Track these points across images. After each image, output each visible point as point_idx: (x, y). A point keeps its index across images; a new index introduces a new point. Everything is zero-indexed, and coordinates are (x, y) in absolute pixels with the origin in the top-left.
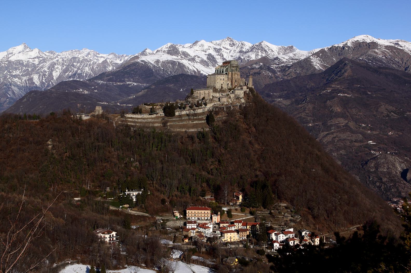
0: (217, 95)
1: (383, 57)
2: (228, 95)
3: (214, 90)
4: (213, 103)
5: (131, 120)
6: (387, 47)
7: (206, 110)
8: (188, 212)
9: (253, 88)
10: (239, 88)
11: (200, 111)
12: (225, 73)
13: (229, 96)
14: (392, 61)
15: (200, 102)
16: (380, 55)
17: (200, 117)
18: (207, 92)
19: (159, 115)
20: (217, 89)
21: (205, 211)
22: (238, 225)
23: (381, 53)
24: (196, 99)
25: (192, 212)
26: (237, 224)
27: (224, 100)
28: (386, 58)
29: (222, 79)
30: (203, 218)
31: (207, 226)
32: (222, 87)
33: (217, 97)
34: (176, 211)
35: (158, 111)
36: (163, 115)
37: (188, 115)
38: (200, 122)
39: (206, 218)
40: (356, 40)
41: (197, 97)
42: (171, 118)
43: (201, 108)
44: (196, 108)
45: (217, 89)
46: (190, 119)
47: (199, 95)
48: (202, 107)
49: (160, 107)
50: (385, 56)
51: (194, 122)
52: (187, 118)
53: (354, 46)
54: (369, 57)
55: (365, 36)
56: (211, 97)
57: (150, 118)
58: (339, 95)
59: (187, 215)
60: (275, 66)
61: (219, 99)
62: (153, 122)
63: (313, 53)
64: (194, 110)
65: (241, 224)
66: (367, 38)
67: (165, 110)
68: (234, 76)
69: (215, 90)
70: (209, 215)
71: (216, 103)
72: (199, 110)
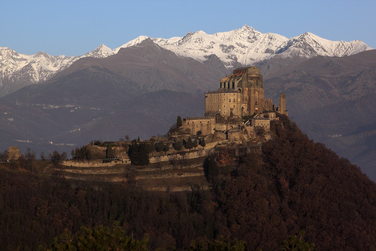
0: (224, 127)
2: (243, 127)
3: (218, 119)
4: (215, 141)
5: (70, 171)
7: (204, 153)
9: (287, 115)
10: (262, 116)
11: (193, 156)
12: (236, 89)
13: (244, 130)
15: (193, 140)
17: (193, 166)
18: (205, 122)
19: (121, 163)
20: (224, 118)
27: (236, 136)
32: (231, 113)
33: (223, 132)
35: (118, 156)
37: (172, 162)
38: (193, 175)
41: (188, 130)
42: (141, 169)
43: (195, 151)
44: (186, 150)
45: (224, 118)
46: (175, 170)
47: (191, 128)
48: (197, 149)
49: (122, 148)
51: (183, 176)
52: (171, 167)
56: (213, 132)
57: (105, 168)
60: (328, 76)
61: (227, 133)
62: (110, 174)
64: (183, 153)
67: (130, 153)
68: (254, 95)
69: (220, 119)
71: (220, 142)
72: (191, 154)
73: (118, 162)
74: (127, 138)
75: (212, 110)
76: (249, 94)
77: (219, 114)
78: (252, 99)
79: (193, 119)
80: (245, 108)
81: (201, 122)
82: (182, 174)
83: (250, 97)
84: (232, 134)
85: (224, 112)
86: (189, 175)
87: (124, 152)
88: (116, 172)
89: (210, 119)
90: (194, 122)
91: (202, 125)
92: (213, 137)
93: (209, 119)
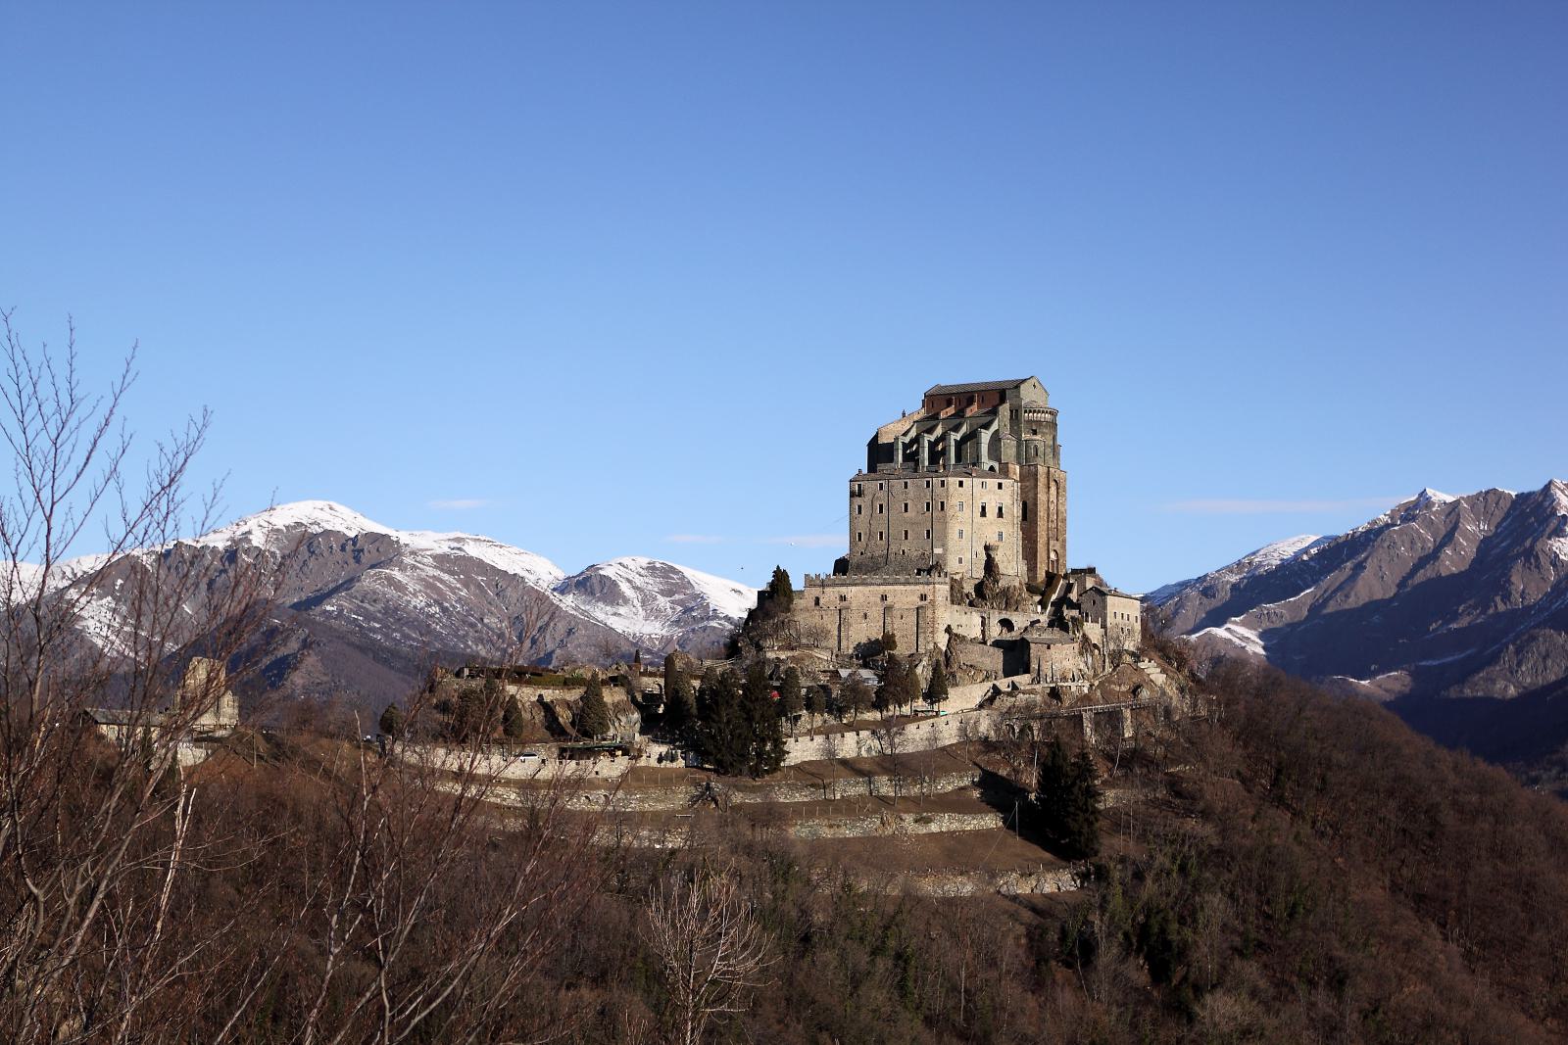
1: (429, 606)
6: (441, 560)
12: (986, 463)
14: (472, 625)
16: (415, 595)
17: (947, 785)
18: (904, 596)
23: (418, 587)
24: (817, 653)
28: (444, 610)
29: (992, 512)
32: (990, 566)
36: (680, 763)
40: (290, 522)
50: (441, 605)
51: (934, 828)
53: (285, 547)
54: (364, 605)
55: (320, 504)
56: (943, 640)
63: (75, 575)
66: (330, 518)
73: (642, 762)
75: (893, 548)
76: (1026, 493)
78: (1042, 514)
79: (842, 585)
81: (884, 598)
82: (928, 821)
83: (1036, 505)
84: (1049, 648)
85: (960, 561)
86: (955, 826)
87: (633, 714)
88: (660, 801)
89: (932, 586)
90: (848, 597)
91: (888, 609)
93: (928, 584)
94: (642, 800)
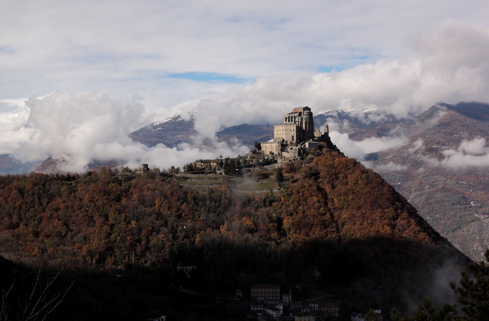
8: (253, 291)
20: (287, 142)
21: (274, 290)
22: (314, 306)
25: (257, 291)
26: (313, 305)
29: (292, 130)
30: (271, 298)
31: (276, 307)
32: (293, 139)
34: (238, 290)
39: (274, 298)
42: (231, 178)
58: (434, 146)
59: (252, 294)
65: (317, 305)
70: (279, 295)
74: (221, 157)
77: (283, 141)
80: (301, 135)
82: (258, 181)
92: (279, 156)
94: (211, 180)
